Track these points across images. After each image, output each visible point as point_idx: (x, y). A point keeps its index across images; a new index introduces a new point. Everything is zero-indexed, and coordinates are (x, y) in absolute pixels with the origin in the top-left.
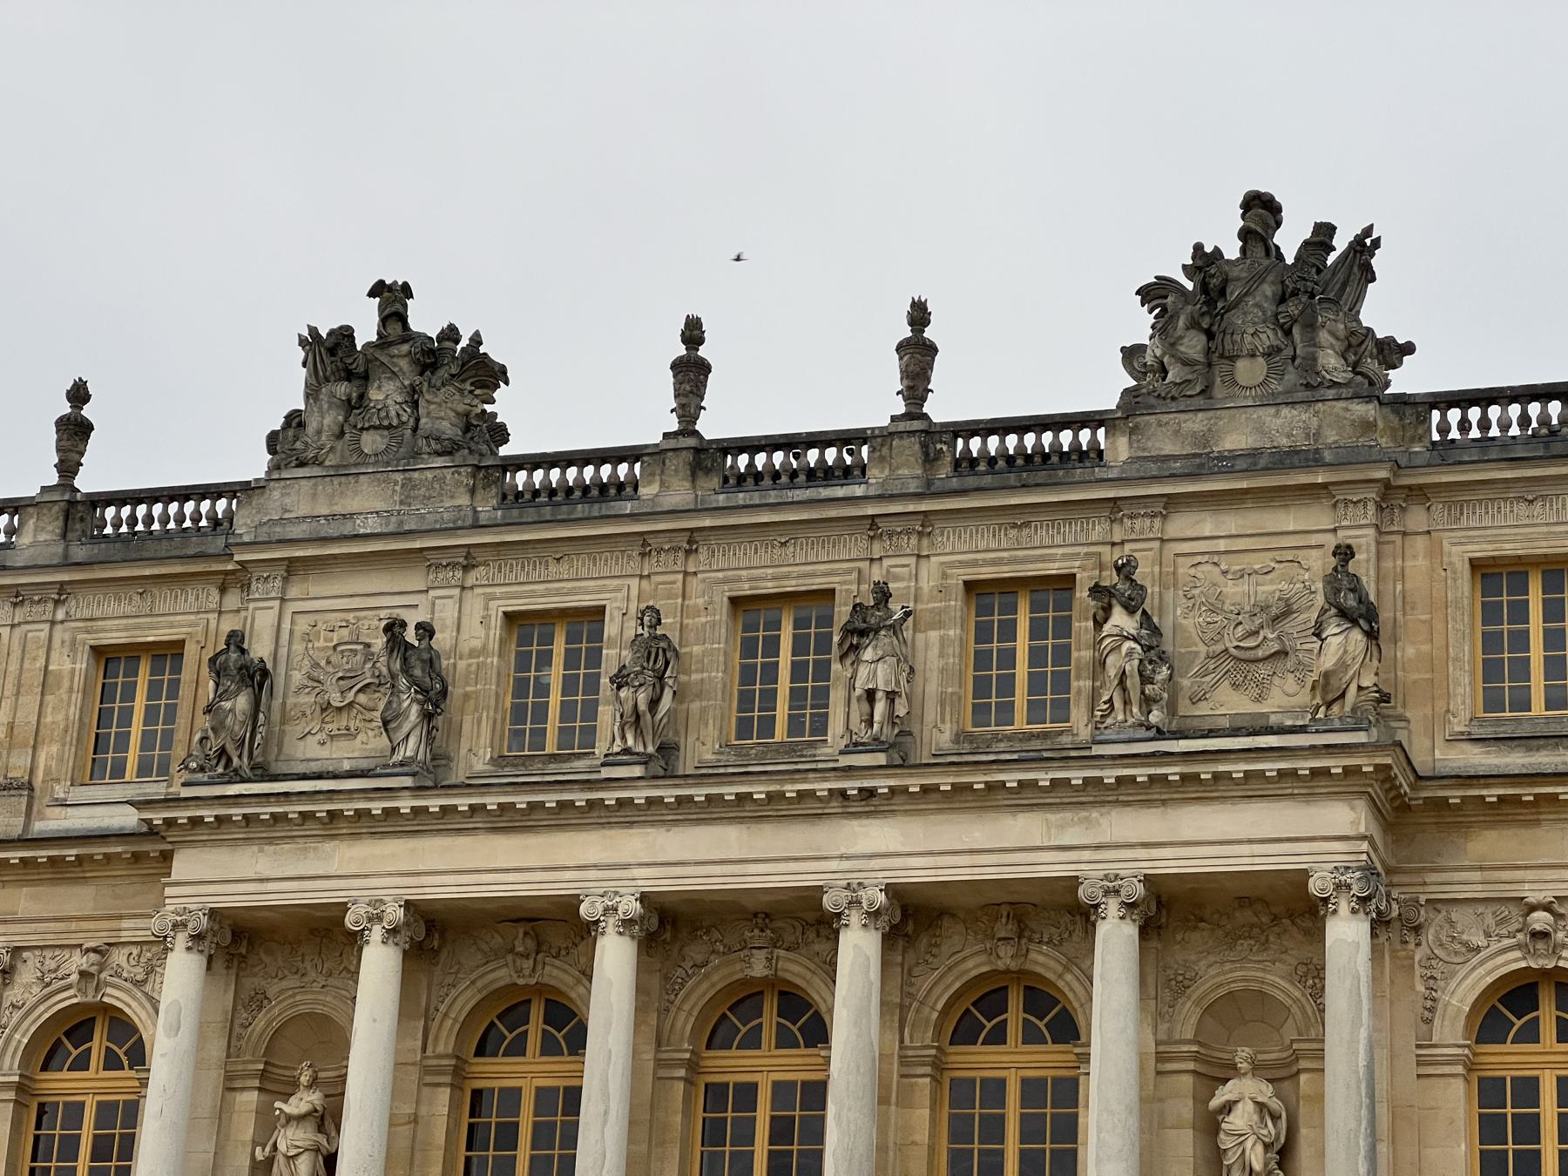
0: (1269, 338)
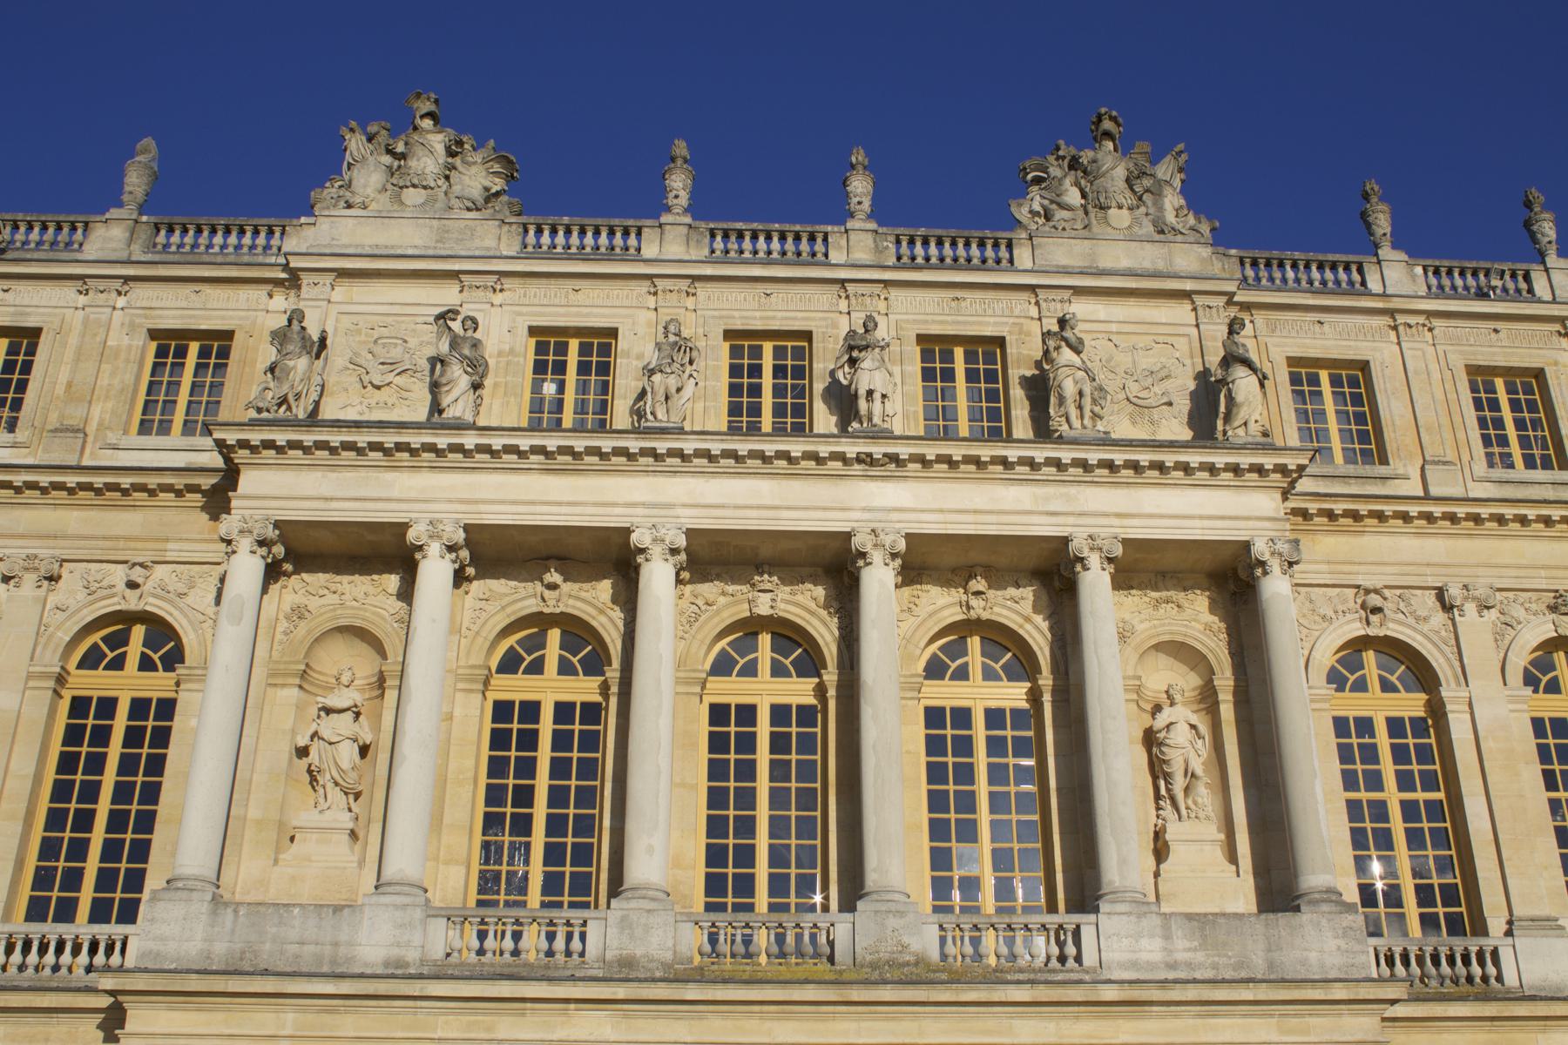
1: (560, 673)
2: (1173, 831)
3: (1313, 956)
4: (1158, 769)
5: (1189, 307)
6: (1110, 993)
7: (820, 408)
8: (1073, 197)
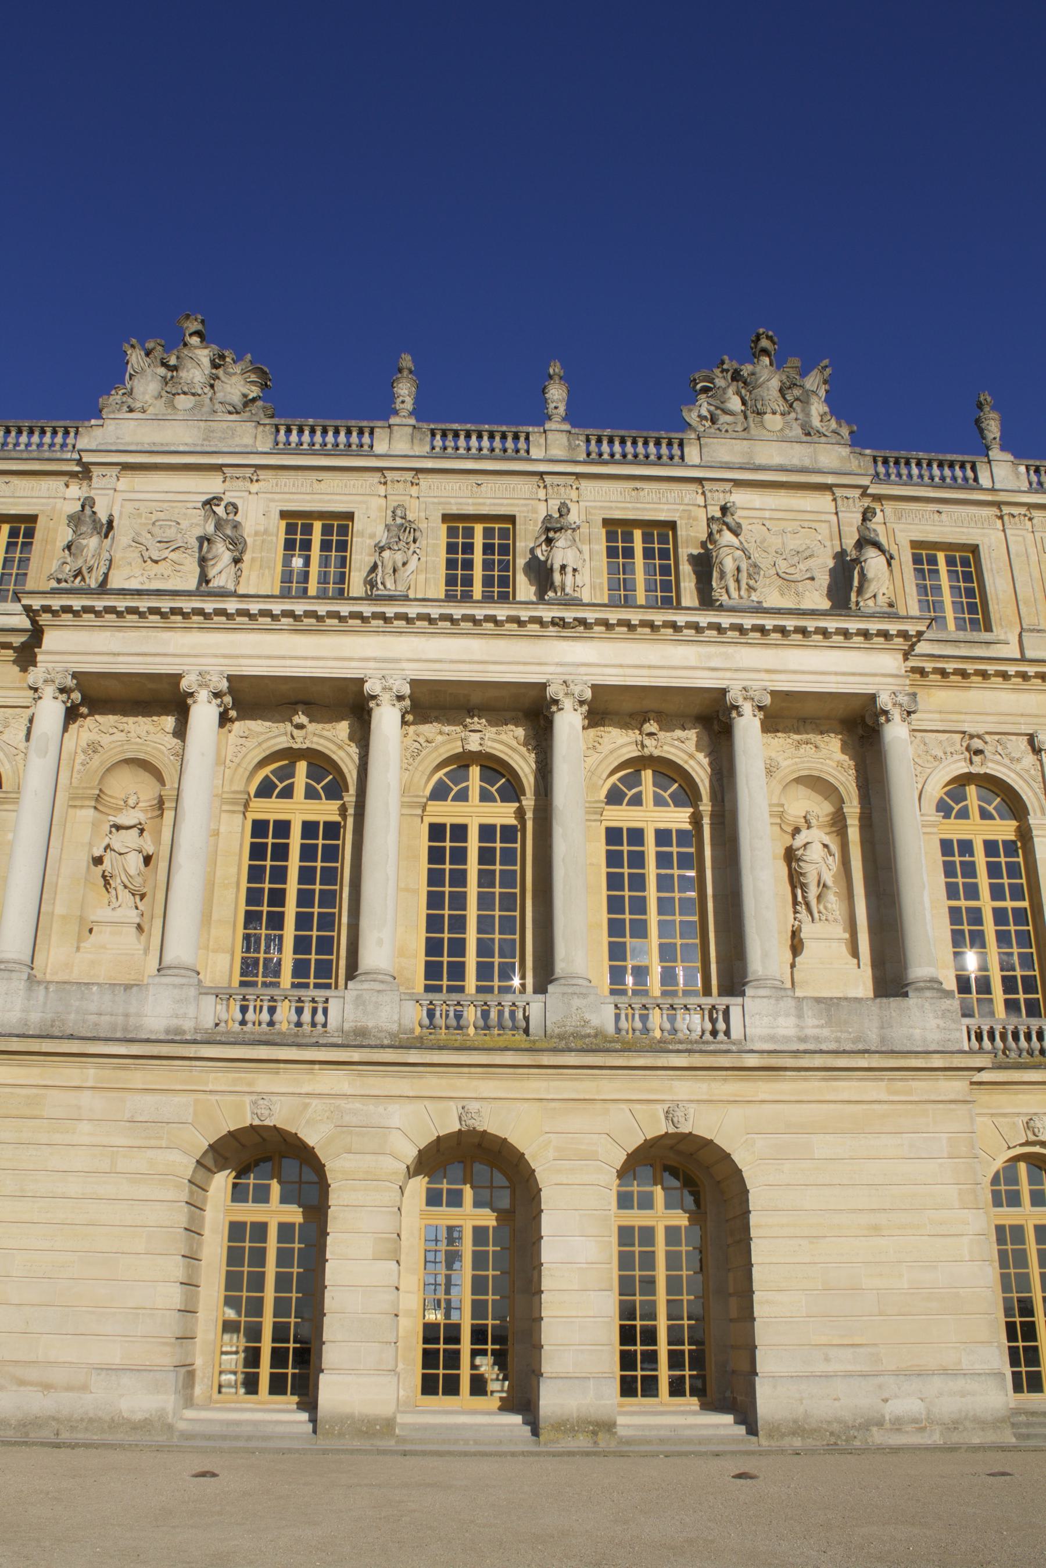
0: (782, 406)
1: (306, 798)
2: (807, 931)
3: (917, 1032)
4: (796, 880)
5: (831, 498)
6: (752, 1061)
7: (521, 580)
8: (735, 404)
